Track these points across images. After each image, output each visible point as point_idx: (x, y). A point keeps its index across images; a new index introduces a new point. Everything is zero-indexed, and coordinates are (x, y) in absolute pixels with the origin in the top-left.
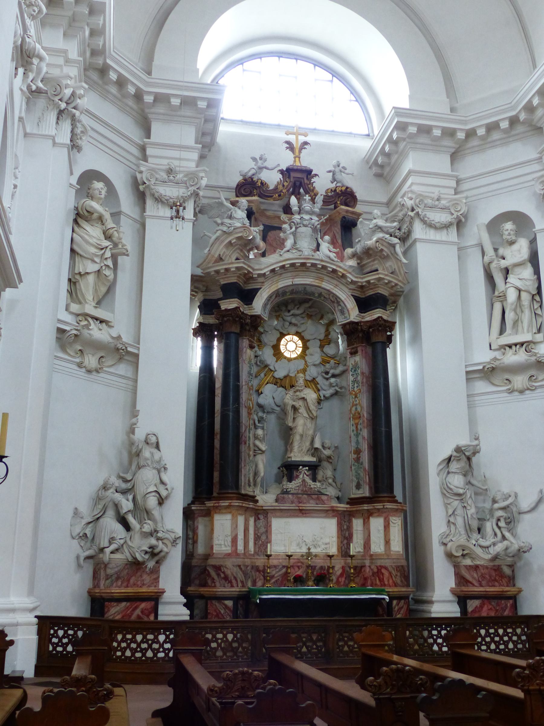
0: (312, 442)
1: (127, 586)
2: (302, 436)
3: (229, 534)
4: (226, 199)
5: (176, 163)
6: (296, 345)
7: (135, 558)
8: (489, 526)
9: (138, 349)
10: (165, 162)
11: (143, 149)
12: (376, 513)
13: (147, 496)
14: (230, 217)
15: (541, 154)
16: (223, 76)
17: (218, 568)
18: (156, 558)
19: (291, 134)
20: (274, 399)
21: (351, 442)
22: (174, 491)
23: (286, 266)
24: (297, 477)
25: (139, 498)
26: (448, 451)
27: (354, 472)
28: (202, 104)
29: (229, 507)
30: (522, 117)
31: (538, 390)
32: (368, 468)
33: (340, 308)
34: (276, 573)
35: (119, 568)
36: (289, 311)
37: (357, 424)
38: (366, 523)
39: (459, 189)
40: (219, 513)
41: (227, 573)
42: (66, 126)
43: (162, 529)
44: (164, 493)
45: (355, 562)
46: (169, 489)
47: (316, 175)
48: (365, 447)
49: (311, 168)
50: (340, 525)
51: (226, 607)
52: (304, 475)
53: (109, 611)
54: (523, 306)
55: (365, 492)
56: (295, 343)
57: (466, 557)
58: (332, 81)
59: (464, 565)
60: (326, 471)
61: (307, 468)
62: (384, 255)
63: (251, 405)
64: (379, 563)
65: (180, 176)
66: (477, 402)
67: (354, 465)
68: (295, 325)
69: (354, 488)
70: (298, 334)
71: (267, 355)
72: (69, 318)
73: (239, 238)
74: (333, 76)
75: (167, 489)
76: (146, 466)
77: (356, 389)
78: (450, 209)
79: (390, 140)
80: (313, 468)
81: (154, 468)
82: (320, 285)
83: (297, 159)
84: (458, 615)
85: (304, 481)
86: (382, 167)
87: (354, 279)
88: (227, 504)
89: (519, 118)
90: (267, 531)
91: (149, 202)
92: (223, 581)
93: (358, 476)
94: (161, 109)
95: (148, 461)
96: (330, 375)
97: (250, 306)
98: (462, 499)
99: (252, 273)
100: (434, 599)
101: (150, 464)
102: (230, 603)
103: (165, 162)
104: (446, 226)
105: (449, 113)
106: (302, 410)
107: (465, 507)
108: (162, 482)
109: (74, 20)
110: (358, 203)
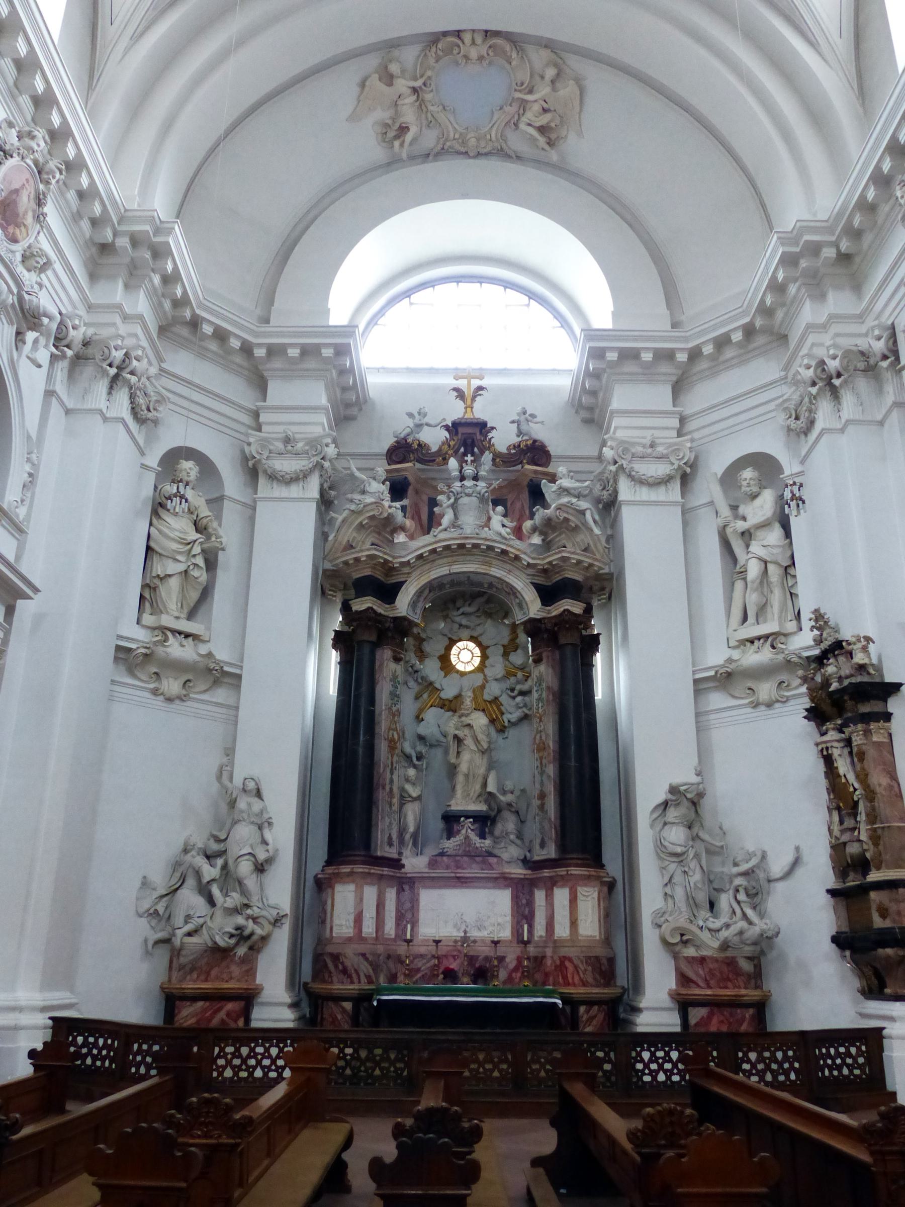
0: (485, 785)
1: (206, 980)
2: (467, 776)
3: (352, 910)
4: (358, 469)
5: (295, 429)
6: (473, 654)
7: (215, 943)
8: (725, 901)
9: (241, 667)
10: (280, 429)
11: (256, 415)
13: (239, 860)
14: (363, 492)
15: (785, 371)
16: (384, 315)
17: (336, 958)
18: (249, 943)
19: (460, 378)
20: (439, 727)
24: (459, 832)
25: (231, 862)
26: (661, 795)
27: (538, 824)
28: (327, 352)
29: (351, 874)
30: (758, 323)
31: (792, 702)
32: (555, 818)
33: (517, 601)
34: (424, 964)
35: (195, 956)
36: (458, 609)
37: (541, 758)
38: (549, 897)
40: (340, 882)
41: (346, 964)
42: (122, 397)
43: (260, 905)
45: (531, 950)
47: (493, 428)
48: (550, 789)
50: (515, 899)
51: (344, 1010)
52: (467, 830)
53: (179, 1012)
54: (772, 583)
55: (551, 852)
56: (471, 651)
57: (688, 945)
58: (528, 305)
59: (684, 957)
60: (508, 824)
61: (471, 820)
63: (396, 736)
64: (564, 952)
65: (300, 445)
66: (713, 722)
67: (538, 815)
68: (467, 627)
69: (538, 847)
70: (472, 639)
71: (431, 669)
72: (141, 635)
73: (372, 518)
74: (530, 298)
75: (268, 851)
76: (240, 821)
77: (540, 710)
79: (588, 374)
81: (253, 823)
82: (487, 572)
83: (469, 409)
84: (678, 1029)
85: (467, 837)
86: (591, 409)
87: (531, 561)
88: (348, 870)
89: (754, 325)
90: (413, 907)
91: (262, 480)
92: (341, 976)
93: (542, 831)
94: (277, 364)
96: (516, 692)
97: (392, 605)
98: (682, 861)
99: (391, 562)
100: (642, 1005)
101: (246, 817)
102: (348, 1005)
104: (665, 481)
105: (670, 329)
106: (469, 742)
107: (685, 872)
108: (265, 842)
109: (135, 267)
110: (553, 460)
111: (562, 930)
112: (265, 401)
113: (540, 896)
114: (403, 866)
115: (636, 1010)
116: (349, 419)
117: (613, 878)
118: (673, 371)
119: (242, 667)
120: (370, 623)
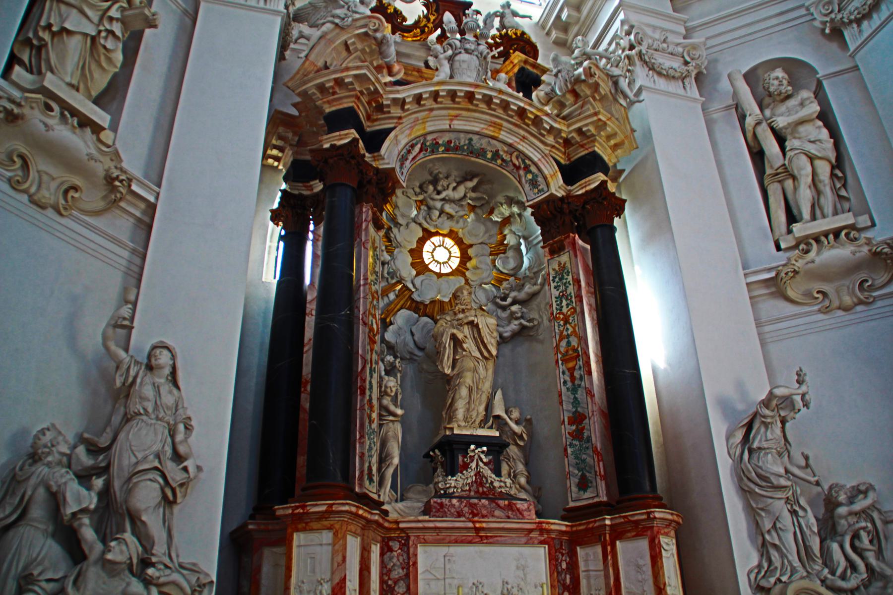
0: (489, 407)
2: (470, 390)
3: (328, 576)
6: (450, 253)
12: (629, 531)
21: (561, 403)
22: (202, 475)
24: (466, 466)
25: (117, 484)
27: (571, 457)
29: (329, 512)
31: (879, 304)
33: (530, 176)
36: (439, 193)
37: (572, 370)
38: (609, 556)
40: (304, 530)
43: (167, 560)
44: (175, 473)
46: (191, 469)
50: (553, 560)
54: (820, 181)
55: (600, 493)
56: (448, 250)
61: (485, 449)
66: (768, 336)
67: (571, 445)
68: (450, 217)
69: (574, 489)
70: (452, 234)
75: (185, 469)
76: (141, 414)
77: (565, 310)
80: (496, 448)
82: (496, 135)
85: (478, 474)
88: (324, 508)
90: (407, 575)
93: (581, 464)
95: (146, 404)
96: (509, 300)
97: (376, 154)
99: (381, 96)
101: (150, 410)
108: (178, 457)
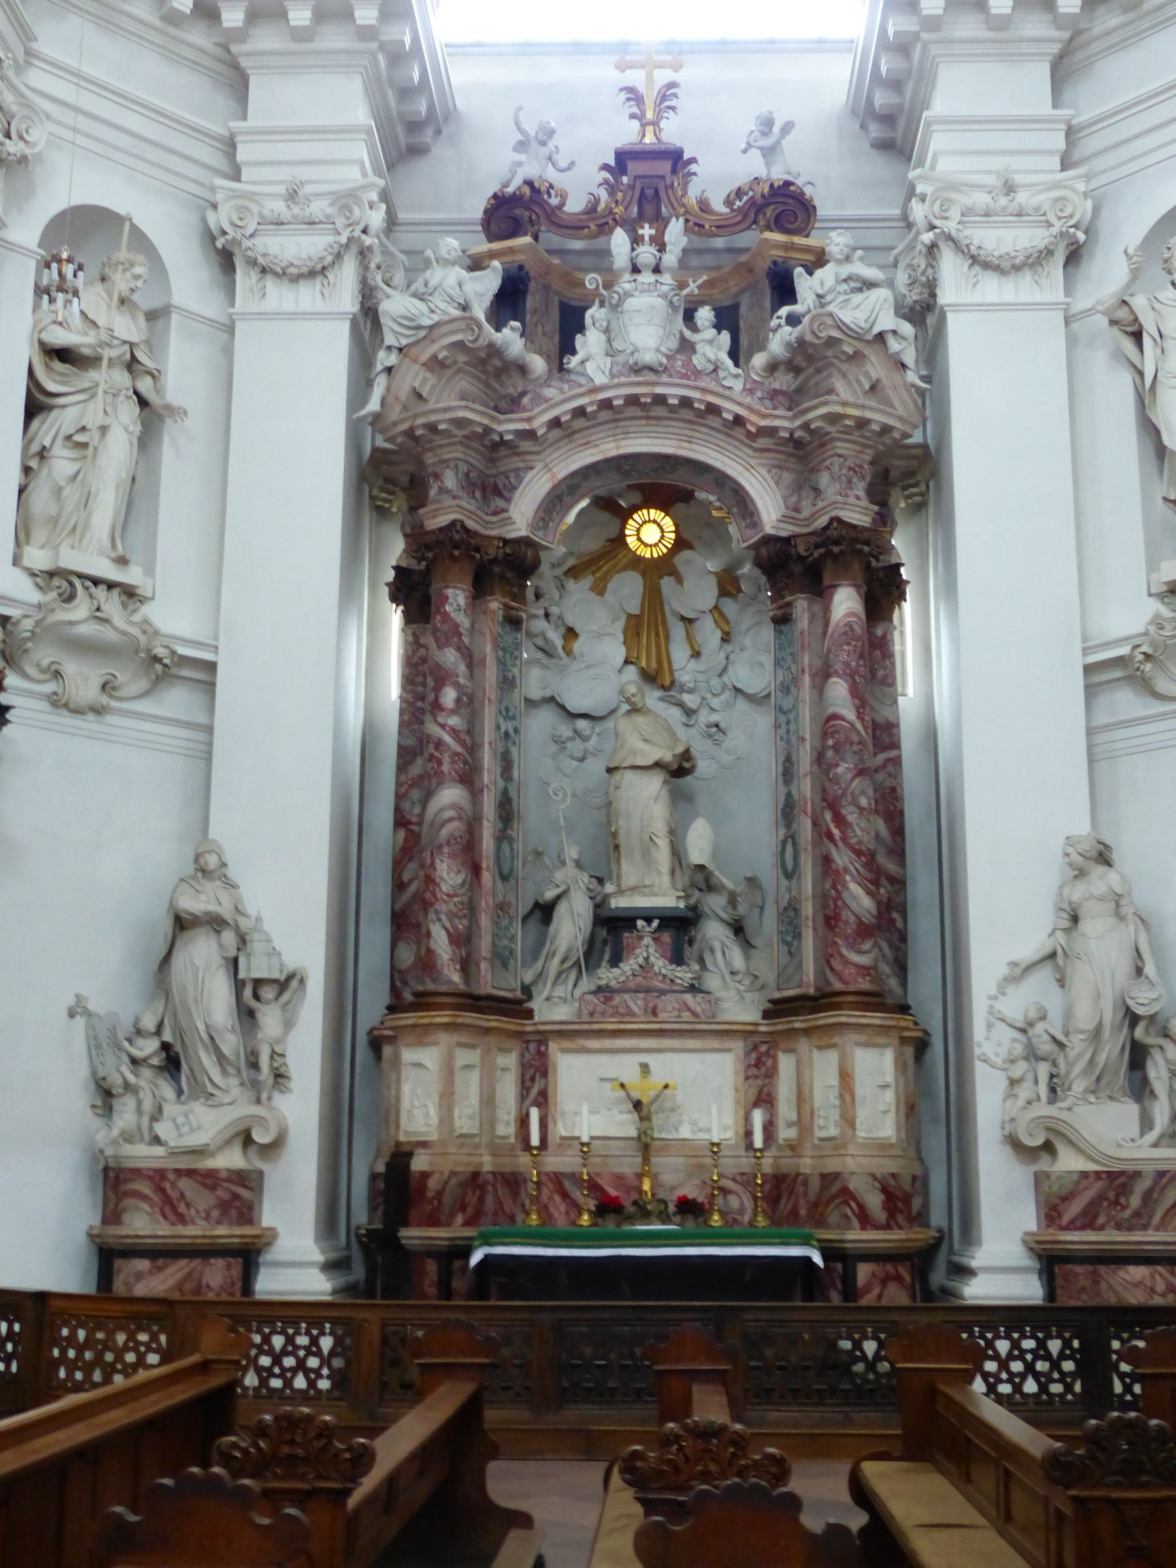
23: (589, 409)
39: (1077, 155)
47: (693, 160)
49: (678, 145)
62: (844, 353)
78: (1044, 214)
79: (884, 44)
84: (1038, 1301)
86: (888, 119)
91: (244, 279)
100: (974, 1264)
103: (283, 173)
104: (1036, 261)
111: (828, 1125)
112: (245, 118)
113: (786, 1064)
114: (529, 1014)
115: (964, 1272)
116: (416, 151)
117: (925, 1032)
118: (1054, 33)
119: (216, 647)
120: (456, 553)
